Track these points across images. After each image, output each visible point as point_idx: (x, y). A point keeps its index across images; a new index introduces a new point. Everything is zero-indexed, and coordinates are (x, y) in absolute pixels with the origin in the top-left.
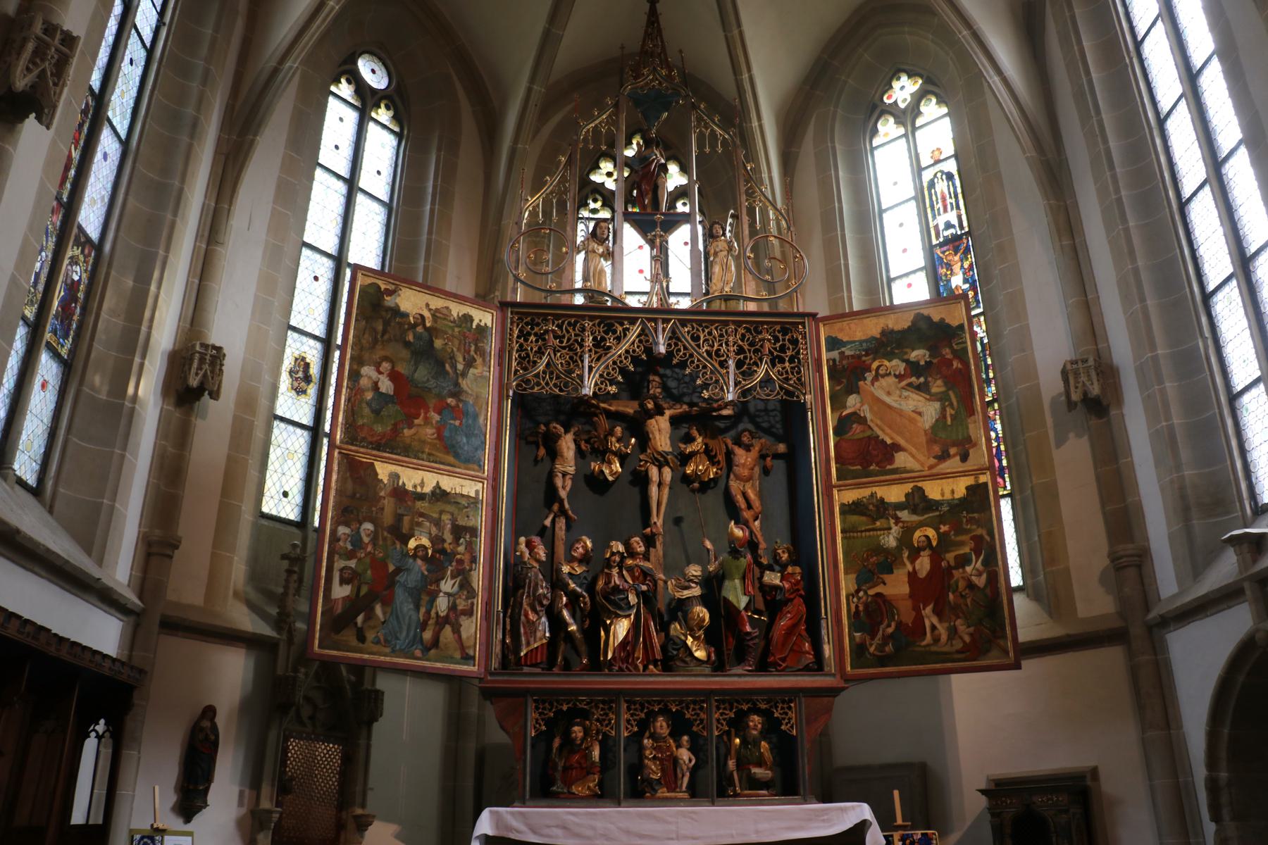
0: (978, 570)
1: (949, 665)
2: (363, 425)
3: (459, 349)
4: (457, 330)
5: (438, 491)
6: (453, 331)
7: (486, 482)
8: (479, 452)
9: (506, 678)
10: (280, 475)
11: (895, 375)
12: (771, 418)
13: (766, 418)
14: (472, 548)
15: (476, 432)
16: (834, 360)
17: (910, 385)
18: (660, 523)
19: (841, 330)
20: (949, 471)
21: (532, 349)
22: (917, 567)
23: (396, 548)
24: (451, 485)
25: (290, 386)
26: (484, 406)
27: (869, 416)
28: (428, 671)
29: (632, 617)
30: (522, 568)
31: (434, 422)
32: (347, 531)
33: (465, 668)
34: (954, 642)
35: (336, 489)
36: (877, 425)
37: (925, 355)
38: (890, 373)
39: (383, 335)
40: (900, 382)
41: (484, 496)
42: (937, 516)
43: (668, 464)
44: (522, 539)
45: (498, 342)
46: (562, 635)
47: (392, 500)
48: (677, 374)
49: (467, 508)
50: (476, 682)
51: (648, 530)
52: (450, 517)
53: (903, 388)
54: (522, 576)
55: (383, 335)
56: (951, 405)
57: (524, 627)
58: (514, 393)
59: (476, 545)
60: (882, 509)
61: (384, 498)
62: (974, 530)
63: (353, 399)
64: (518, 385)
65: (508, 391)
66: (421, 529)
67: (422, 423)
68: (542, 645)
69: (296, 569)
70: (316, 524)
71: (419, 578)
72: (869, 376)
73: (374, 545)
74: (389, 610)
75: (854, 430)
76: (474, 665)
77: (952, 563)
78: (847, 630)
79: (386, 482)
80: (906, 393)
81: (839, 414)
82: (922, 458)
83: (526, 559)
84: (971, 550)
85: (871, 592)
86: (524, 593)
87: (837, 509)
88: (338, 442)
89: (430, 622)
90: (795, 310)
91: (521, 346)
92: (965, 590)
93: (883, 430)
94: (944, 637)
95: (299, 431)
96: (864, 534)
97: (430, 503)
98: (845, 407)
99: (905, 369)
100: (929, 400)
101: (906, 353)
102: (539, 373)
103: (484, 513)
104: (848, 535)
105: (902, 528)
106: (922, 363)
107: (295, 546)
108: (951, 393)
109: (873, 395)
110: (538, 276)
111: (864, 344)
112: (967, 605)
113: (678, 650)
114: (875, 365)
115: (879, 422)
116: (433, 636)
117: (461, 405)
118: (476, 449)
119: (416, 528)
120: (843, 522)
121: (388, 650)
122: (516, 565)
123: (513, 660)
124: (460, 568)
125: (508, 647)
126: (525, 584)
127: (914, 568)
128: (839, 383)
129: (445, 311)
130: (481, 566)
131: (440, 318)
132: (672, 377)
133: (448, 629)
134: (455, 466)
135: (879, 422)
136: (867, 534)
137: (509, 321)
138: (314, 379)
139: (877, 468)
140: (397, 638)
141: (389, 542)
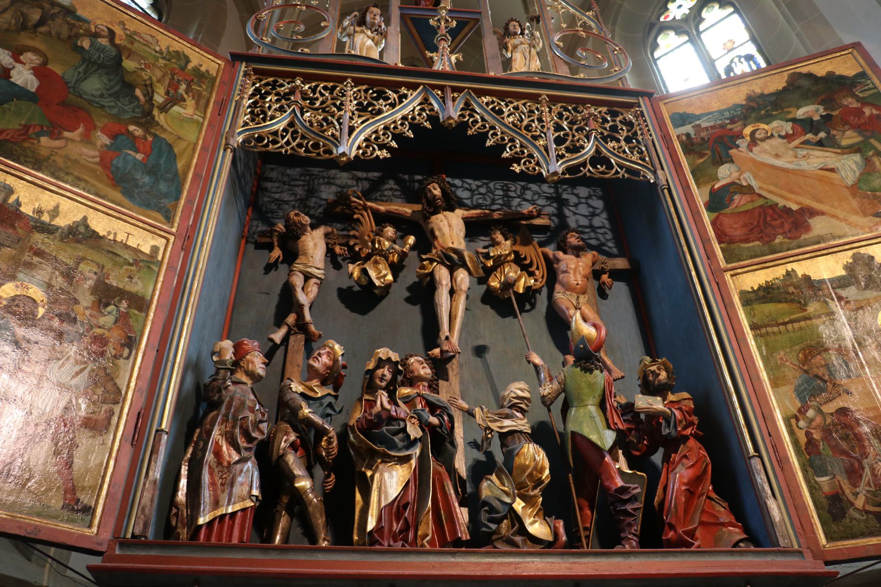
12: (600, 236)
13: (592, 235)
18: (455, 339)
27: (754, 183)
29: (413, 462)
37: (818, 110)
41: (165, 256)
43: (464, 265)
46: (285, 500)
48: (469, 184)
51: (437, 351)
57: (211, 473)
68: (244, 510)
72: (743, 144)
75: (736, 202)
85: (830, 408)
86: (218, 415)
93: (781, 196)
96: (789, 327)
99: (793, 128)
100: (843, 154)
104: (763, 331)
109: (754, 161)
113: (499, 521)
114: (748, 131)
120: (749, 315)
132: (462, 187)
135: (772, 188)
136: (796, 325)
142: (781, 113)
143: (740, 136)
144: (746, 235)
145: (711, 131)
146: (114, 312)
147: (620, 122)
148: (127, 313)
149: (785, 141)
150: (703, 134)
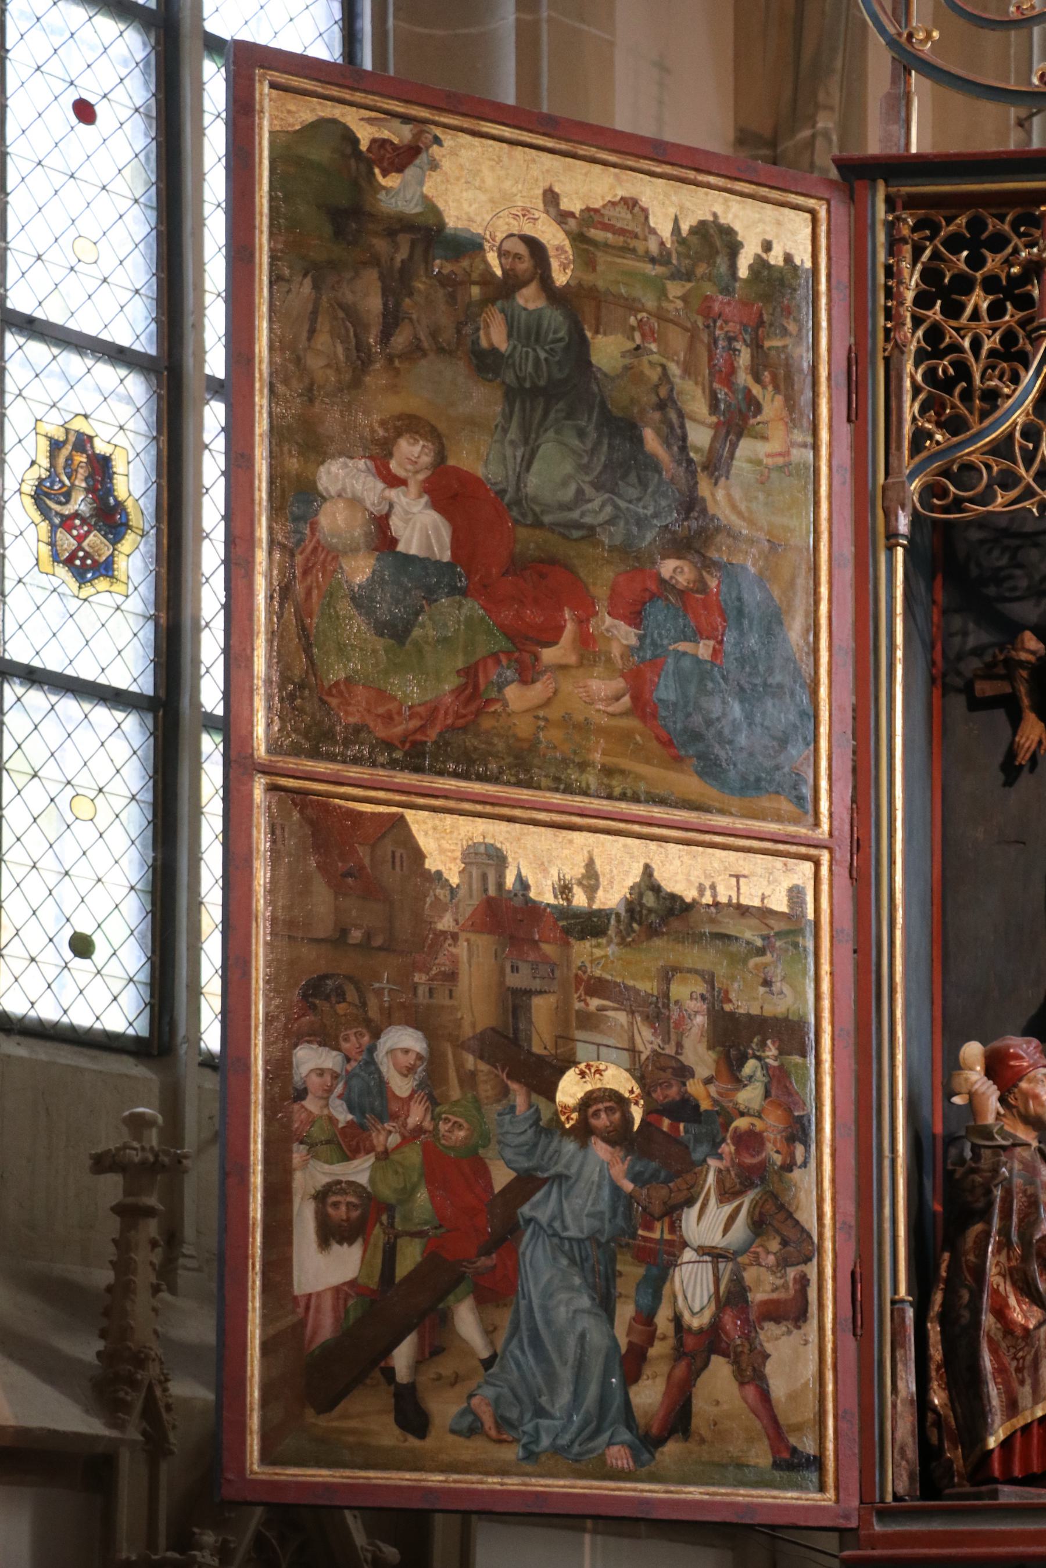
2: (348, 680)
3: (688, 371)
4: (675, 290)
5: (649, 900)
6: (663, 294)
7: (825, 857)
8: (796, 751)
9: (937, 1526)
10: (52, 879)
14: (789, 1092)
15: (777, 678)
21: (976, 344)
23: (513, 1108)
24: (697, 876)
25: (45, 550)
26: (803, 581)
28: (655, 1515)
30: (975, 1148)
31: (616, 651)
32: (329, 1059)
33: (789, 1497)
35: (274, 920)
39: (386, 336)
44: (973, 1051)
45: (843, 325)
47: (484, 942)
49: (761, 952)
50: (830, 1543)
52: (701, 988)
54: (978, 1179)
55: (386, 336)
58: (916, 520)
59: (803, 1080)
61: (455, 937)
63: (299, 588)
64: (930, 491)
65: (887, 513)
66: (598, 1038)
67: (572, 659)
69: (152, 1201)
70: (212, 1039)
71: (604, 1205)
73: (433, 1101)
74: (504, 1318)
76: (822, 1488)
79: (454, 881)
83: (990, 1119)
88: (261, 750)
89: (652, 1352)
91: (934, 334)
95: (103, 716)
97: (623, 943)
102: (1010, 436)
103: (825, 968)
107: (138, 1124)
110: (991, 38)
116: (666, 1394)
117: (713, 583)
118: (783, 742)
119: (579, 1035)
121: (511, 1453)
122: (951, 1140)
123: (959, 1464)
124: (749, 1160)
125: (939, 1422)
126: (990, 1204)
129: (623, 218)
130: (827, 1151)
131: (606, 246)
133: (720, 1369)
134: (707, 810)
137: (881, 237)
138: (135, 519)
140: (540, 1412)
141: (486, 1090)
146: (759, 1073)
148: (781, 1067)
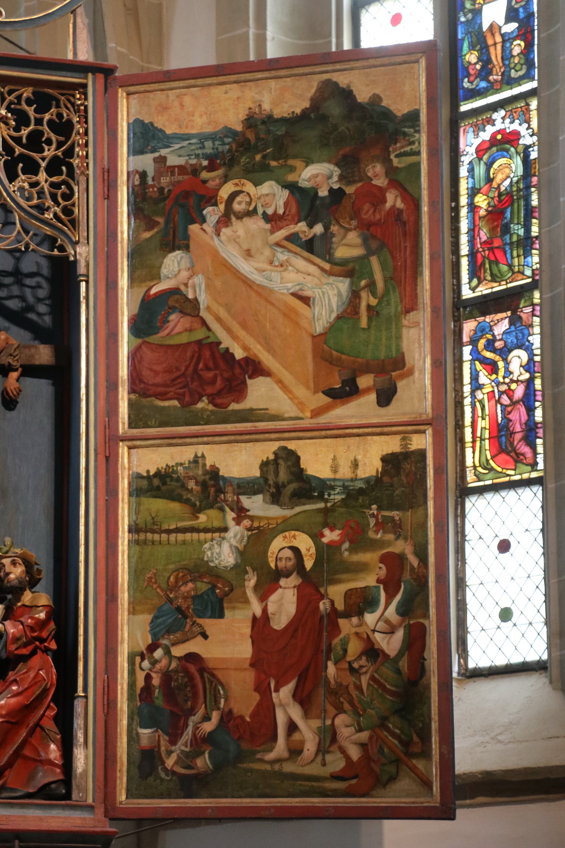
0: (387, 622)
1: (316, 801)
11: (267, 218)
16: (143, 175)
17: (292, 238)
19: (164, 108)
20: (353, 422)
22: (271, 608)
27: (203, 299)
34: (328, 758)
36: (219, 319)
37: (330, 177)
38: (255, 211)
40: (272, 232)
42: (319, 510)
53: (278, 244)
56: (371, 286)
60: (212, 490)
62: (389, 543)
75: (171, 325)
77: (340, 606)
78: (125, 722)
80: (282, 256)
81: (145, 289)
82: (302, 392)
84: (378, 581)
85: (179, 651)
87: (124, 485)
90: (70, 56)
92: (359, 657)
93: (229, 330)
94: (310, 747)
96: (173, 537)
98: (156, 277)
99: (286, 204)
101: (292, 169)
105: (249, 529)
106: (323, 193)
108: (374, 261)
109: (215, 254)
111: (209, 144)
112: (359, 688)
114: (225, 192)
115: (223, 313)
127: (265, 611)
128: (150, 224)
135: (223, 313)
136: (180, 536)
139: (211, 407)
142: (282, 166)
143: (212, 200)
144: (165, 385)
145: (178, 178)
147: (51, 123)
149: (268, 226)
150: (165, 181)
